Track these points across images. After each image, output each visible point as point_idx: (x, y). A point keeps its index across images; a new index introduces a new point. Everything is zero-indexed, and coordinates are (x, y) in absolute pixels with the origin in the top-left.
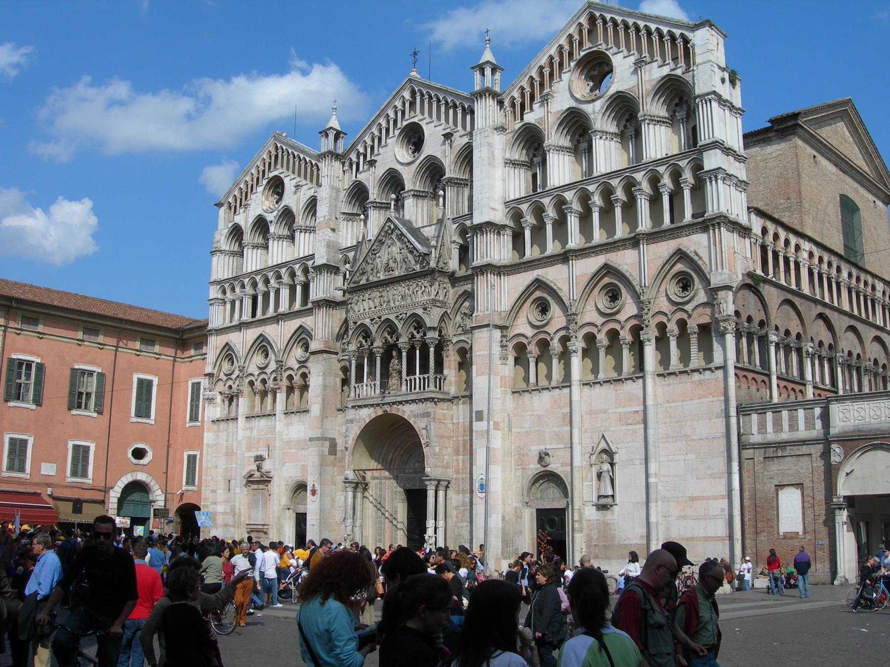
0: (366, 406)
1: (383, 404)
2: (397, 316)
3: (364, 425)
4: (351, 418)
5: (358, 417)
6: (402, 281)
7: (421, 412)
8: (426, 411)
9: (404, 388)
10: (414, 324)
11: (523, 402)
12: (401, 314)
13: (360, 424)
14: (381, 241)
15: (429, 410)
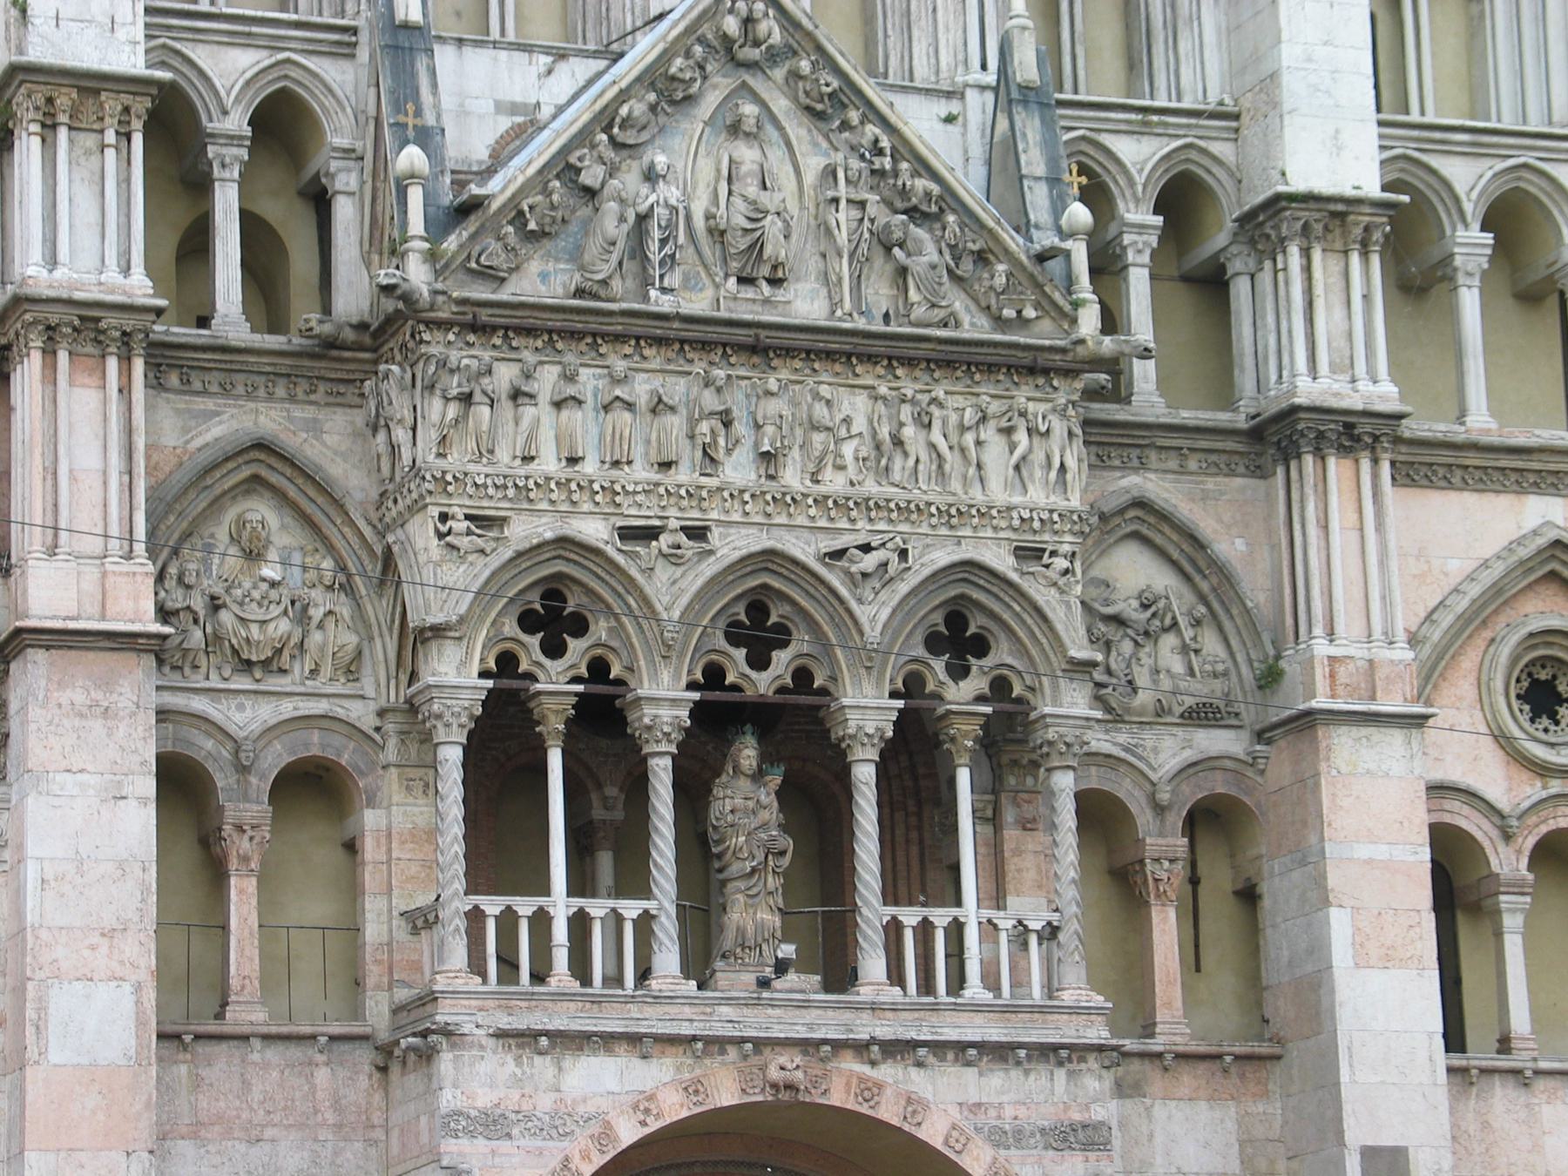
0: (607, 1041)
1: (760, 1044)
2: (839, 554)
3: (599, 1161)
4: (480, 1104)
5: (545, 1102)
6: (871, 359)
7: (1045, 1115)
8: (1077, 1116)
9: (873, 965)
10: (938, 618)
11: (1486, 1125)
12: (866, 548)
13: (573, 1148)
14: (673, 78)
15: (1098, 1113)
